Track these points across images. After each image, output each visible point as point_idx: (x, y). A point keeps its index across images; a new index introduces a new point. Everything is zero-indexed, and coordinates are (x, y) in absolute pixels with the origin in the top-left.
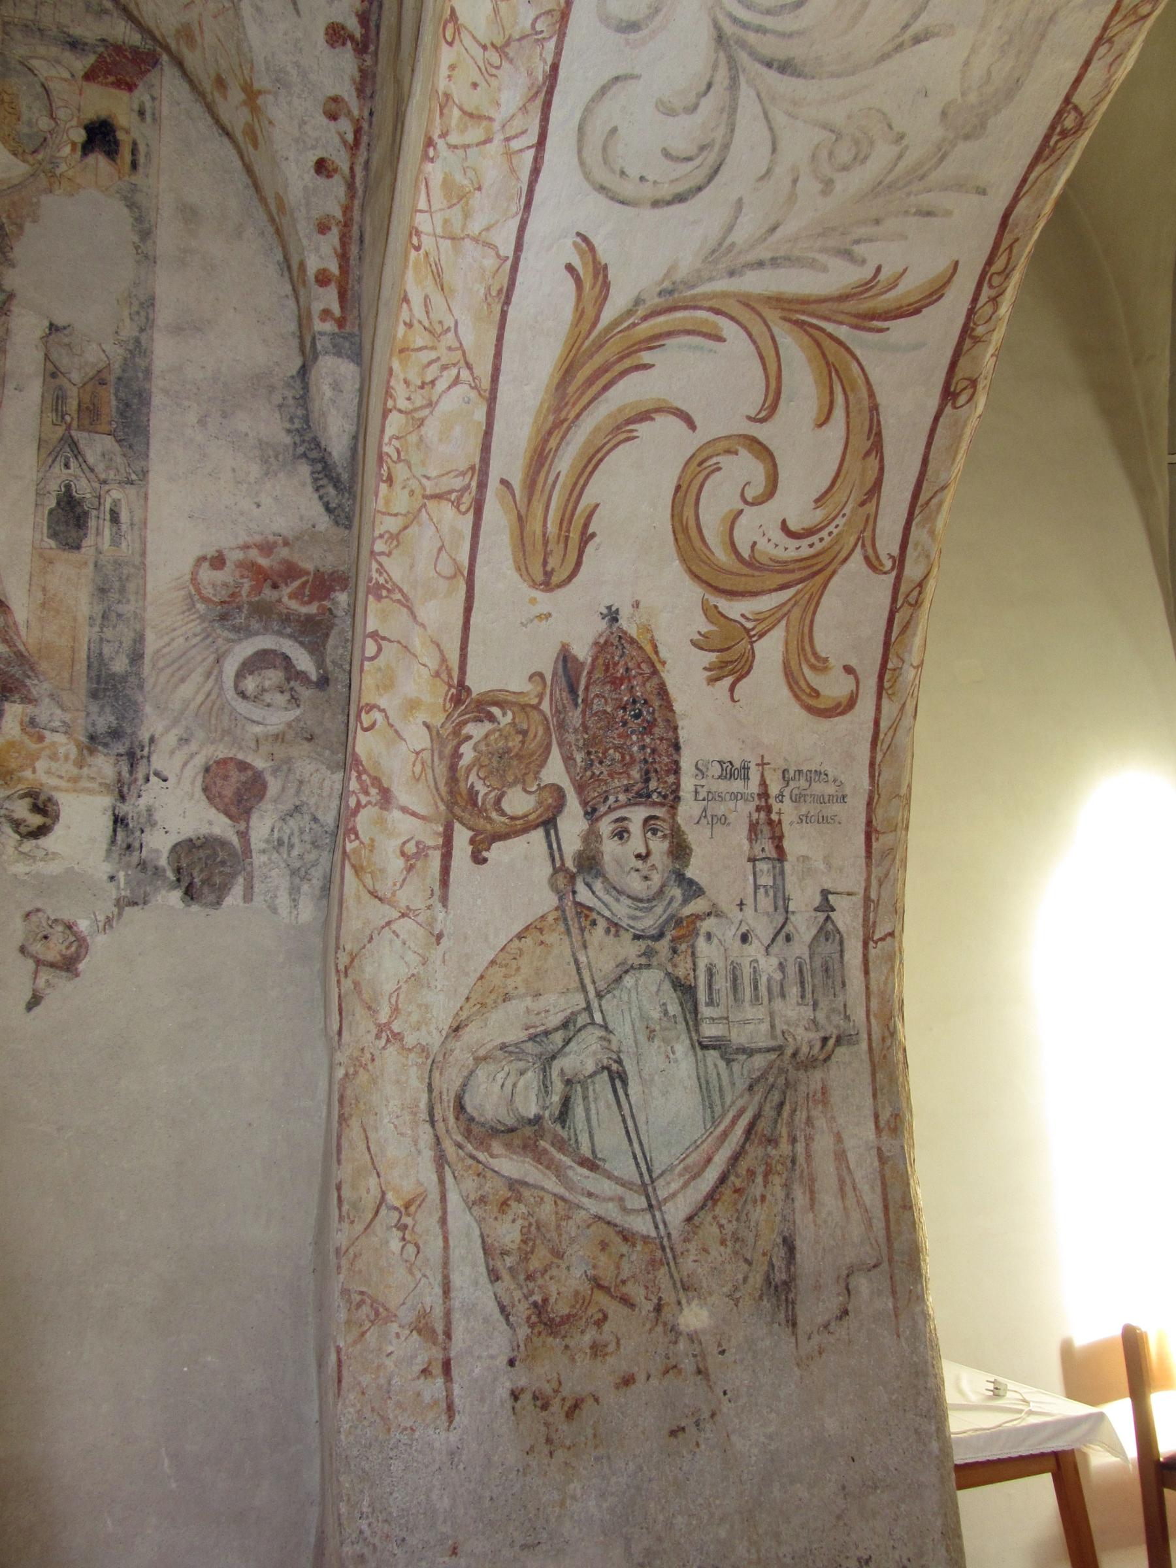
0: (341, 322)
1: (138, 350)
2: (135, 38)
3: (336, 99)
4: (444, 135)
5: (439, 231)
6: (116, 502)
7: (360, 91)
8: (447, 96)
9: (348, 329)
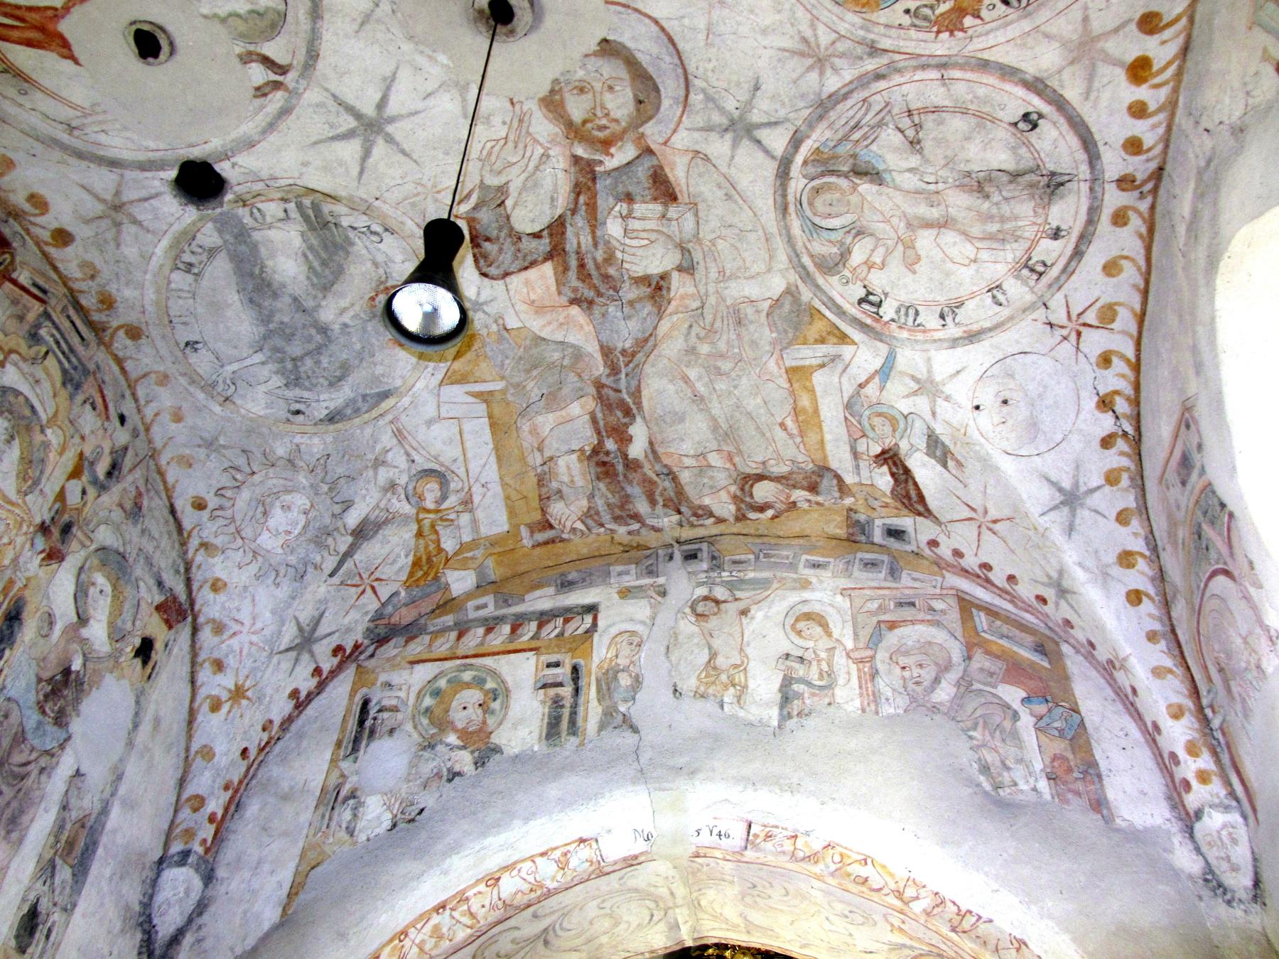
0: (207, 851)
1: (105, 810)
2: (183, 598)
3: (271, 722)
4: (452, 909)
5: (417, 941)
6: (54, 923)
7: (282, 724)
8: (467, 899)
9: (208, 857)
